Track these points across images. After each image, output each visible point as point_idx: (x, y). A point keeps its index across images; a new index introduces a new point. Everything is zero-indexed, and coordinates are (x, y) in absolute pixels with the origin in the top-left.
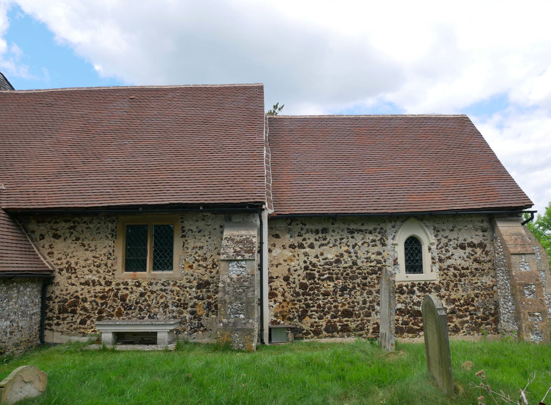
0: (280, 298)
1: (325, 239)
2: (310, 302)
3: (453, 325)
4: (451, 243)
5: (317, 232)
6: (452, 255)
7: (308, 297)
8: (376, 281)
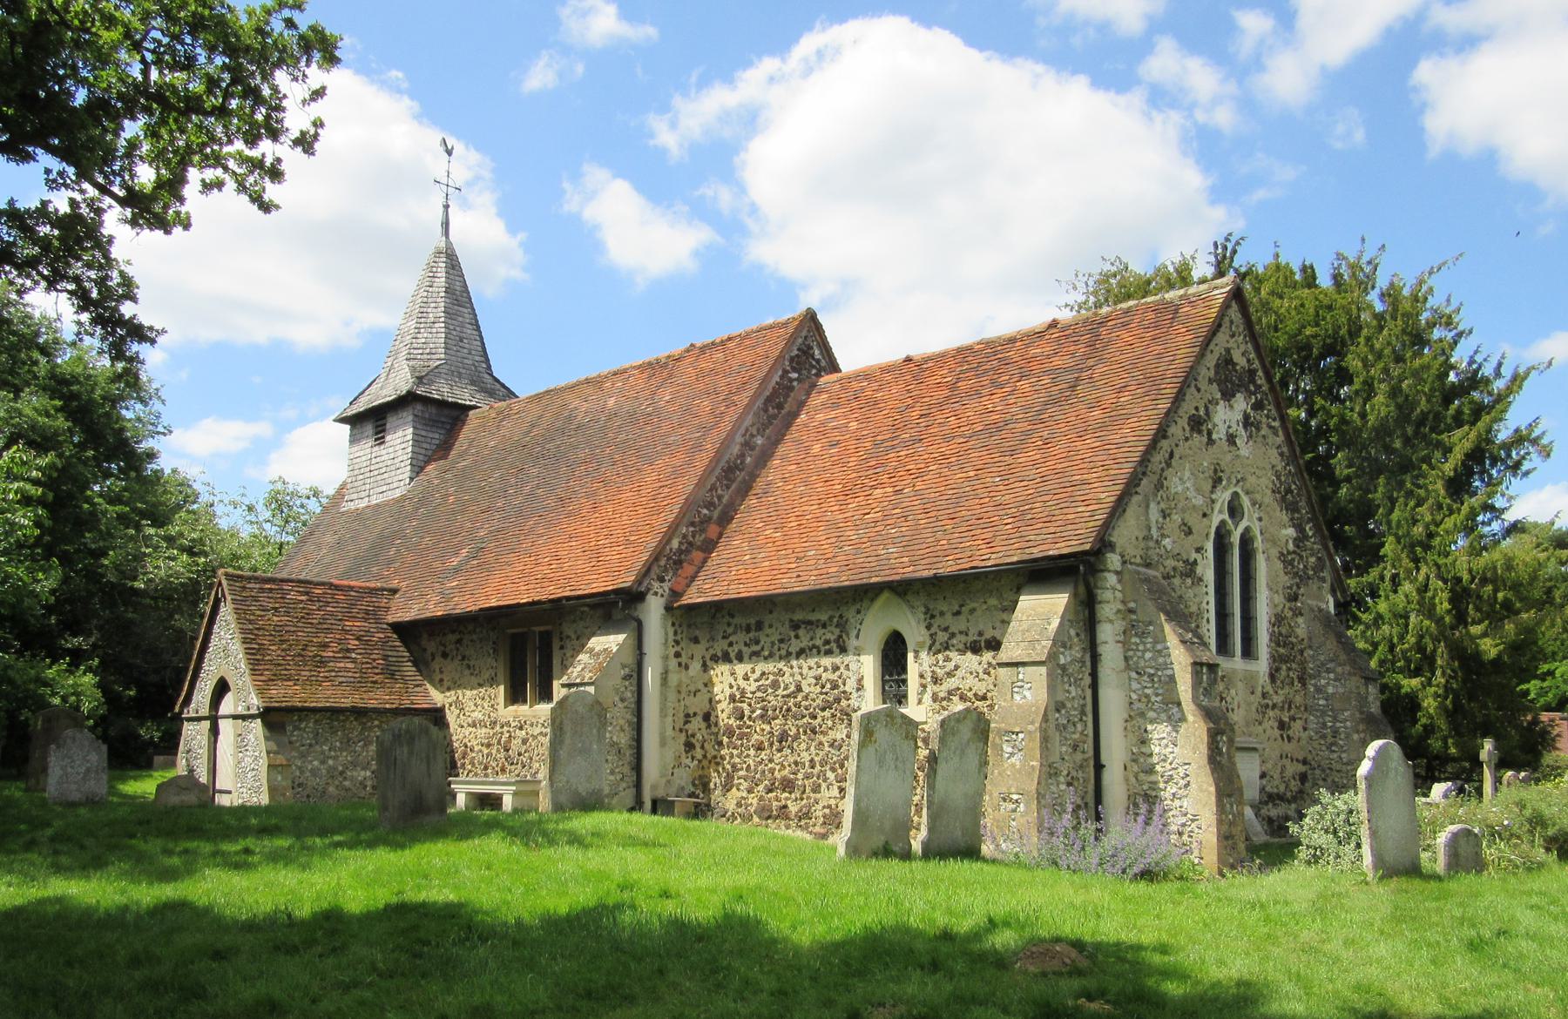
0: (698, 753)
1: (757, 642)
2: (737, 760)
4: (954, 641)
5: (748, 630)
6: (957, 667)
7: (735, 752)
8: (830, 723)
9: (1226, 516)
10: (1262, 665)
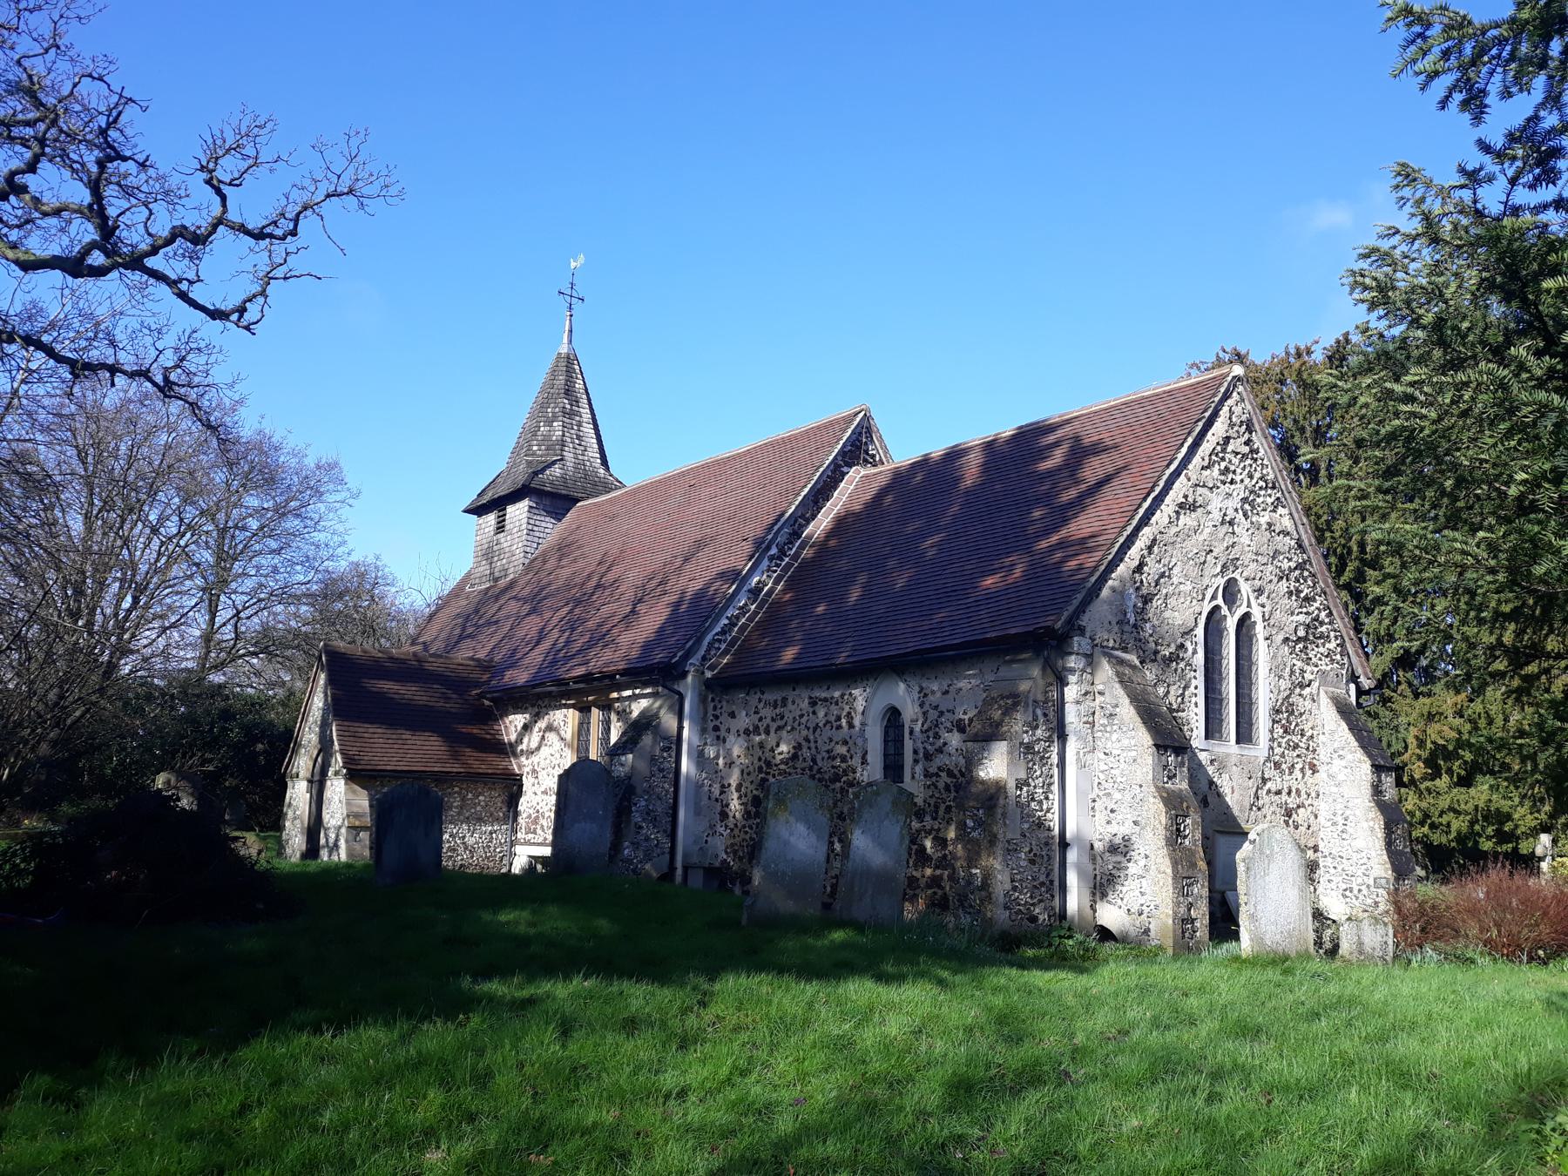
3: (940, 892)
9: (1220, 601)
10: (1260, 749)
